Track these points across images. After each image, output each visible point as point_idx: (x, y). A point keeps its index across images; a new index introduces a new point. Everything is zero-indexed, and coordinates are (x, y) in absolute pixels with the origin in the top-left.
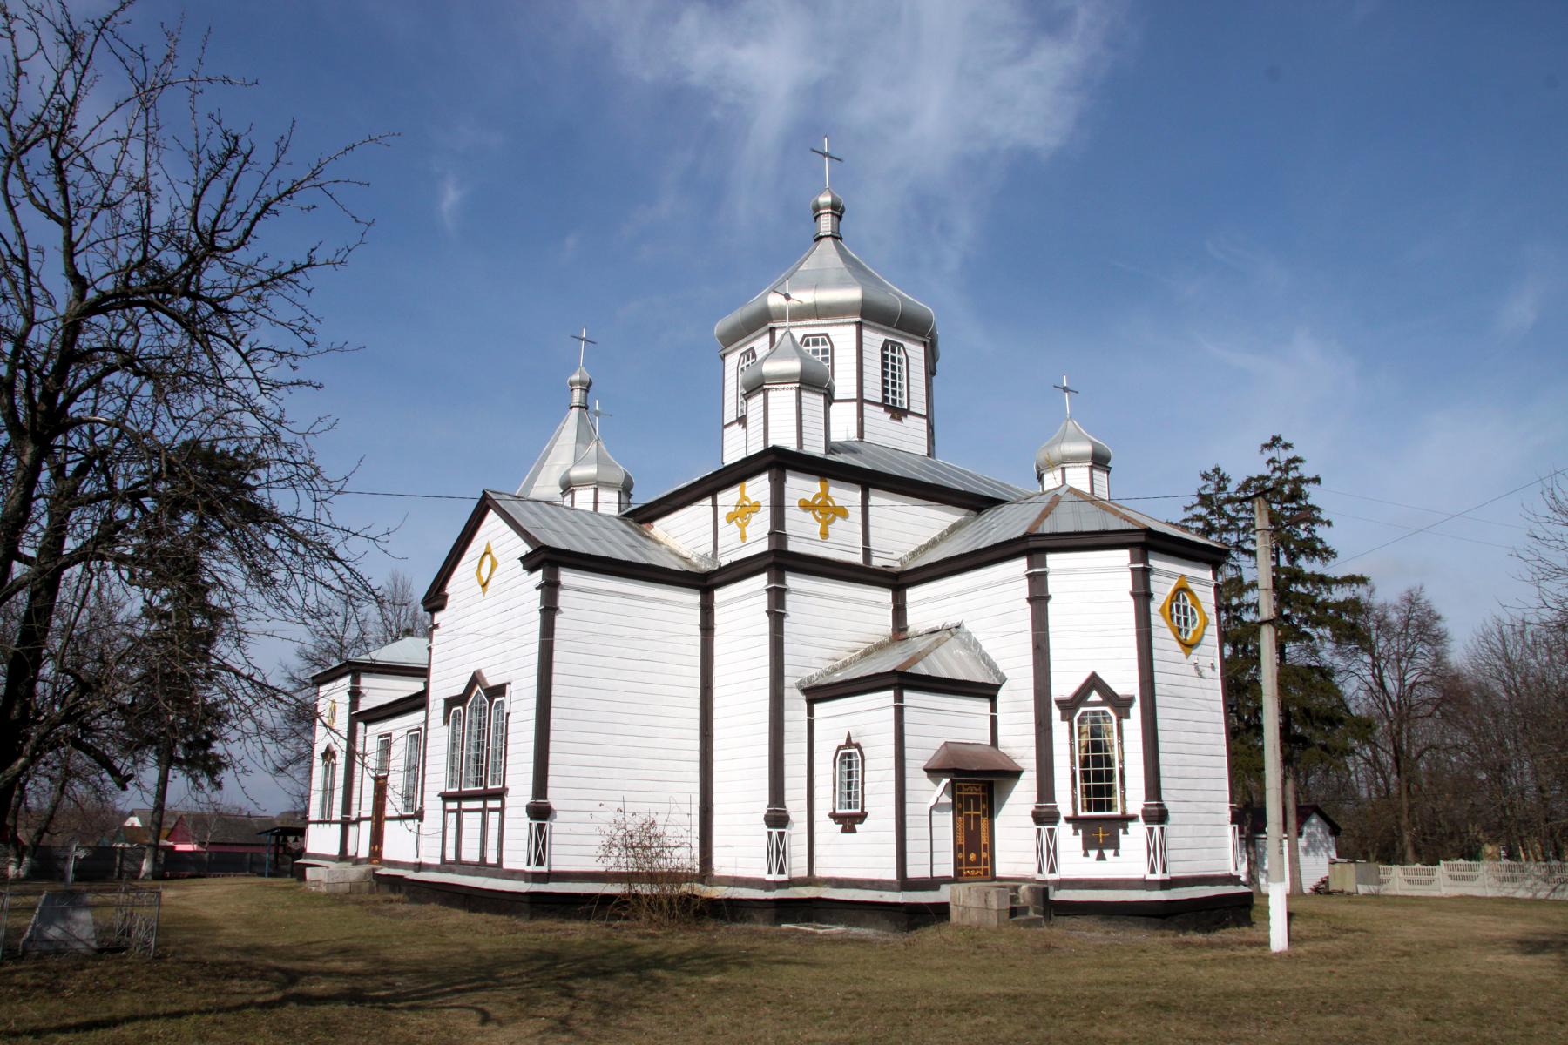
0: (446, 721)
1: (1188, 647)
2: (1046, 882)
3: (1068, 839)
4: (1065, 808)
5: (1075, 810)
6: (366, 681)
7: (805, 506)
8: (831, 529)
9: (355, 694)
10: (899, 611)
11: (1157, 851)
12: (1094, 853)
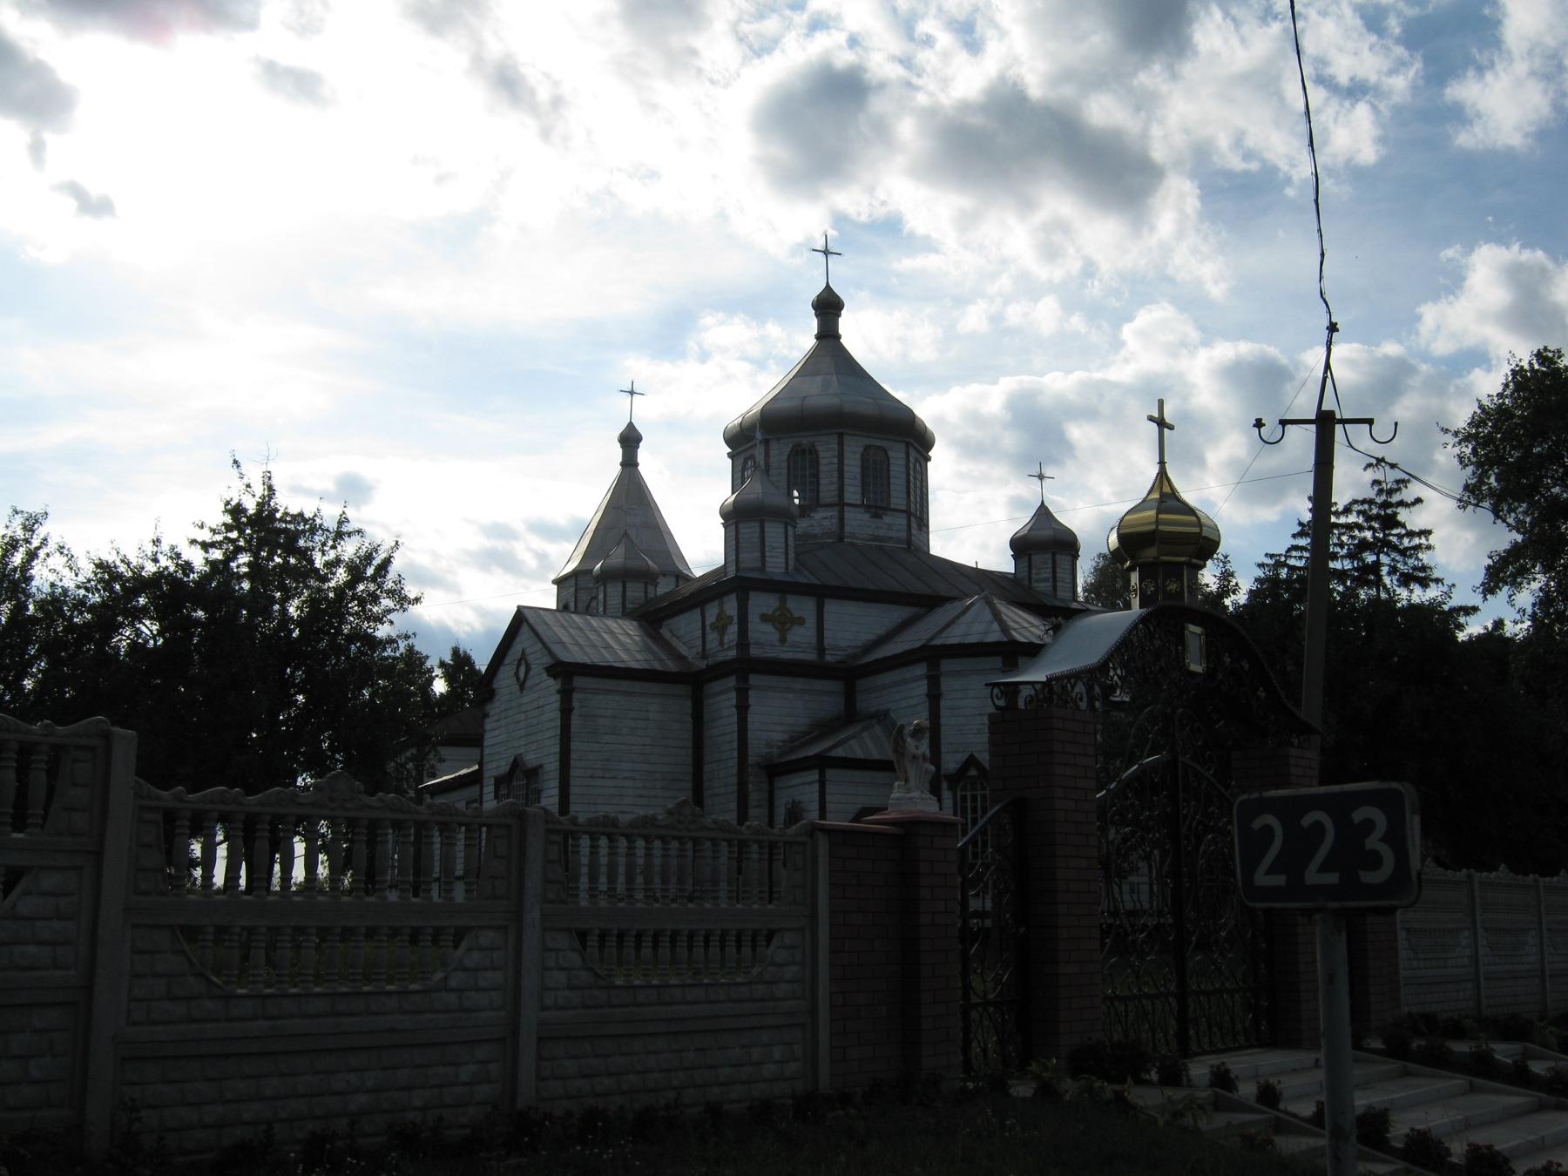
7: (765, 618)
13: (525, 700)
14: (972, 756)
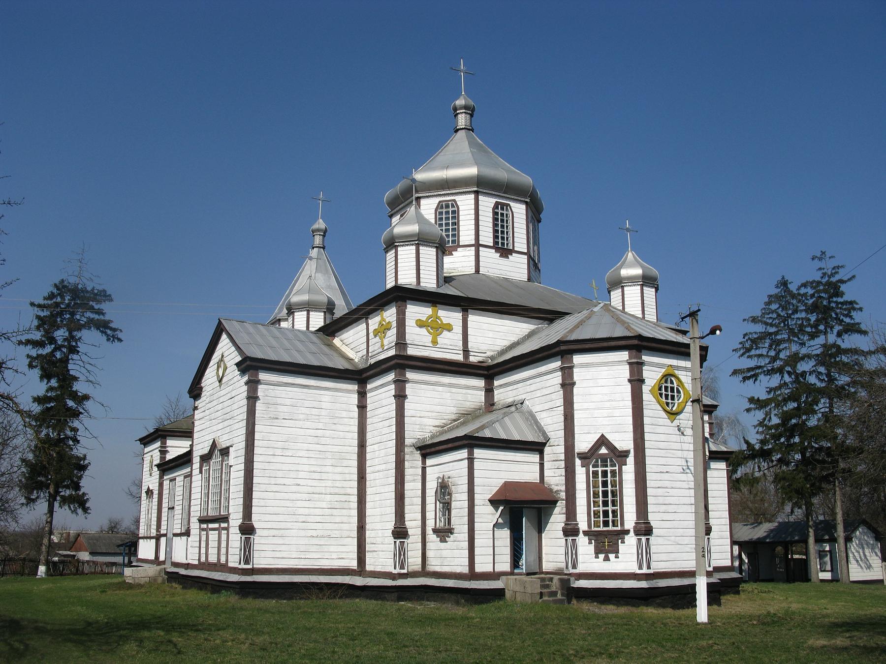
0: (201, 472)
1: (673, 414)
2: (570, 574)
3: (585, 547)
4: (583, 525)
5: (589, 526)
6: (170, 442)
7: (421, 324)
8: (439, 340)
9: (163, 452)
10: (489, 391)
11: (644, 554)
12: (602, 556)
13: (222, 393)
14: (603, 435)
